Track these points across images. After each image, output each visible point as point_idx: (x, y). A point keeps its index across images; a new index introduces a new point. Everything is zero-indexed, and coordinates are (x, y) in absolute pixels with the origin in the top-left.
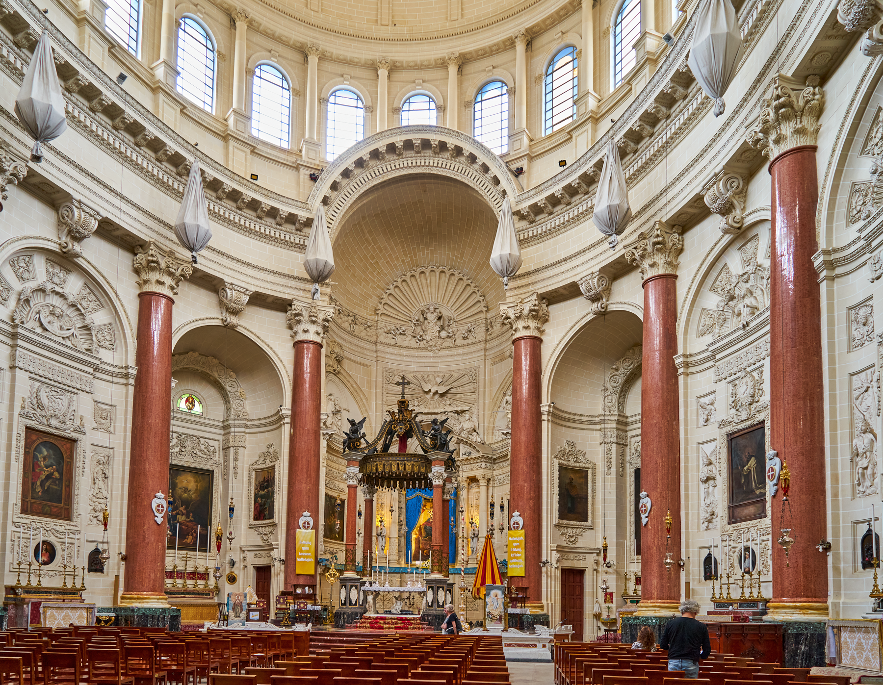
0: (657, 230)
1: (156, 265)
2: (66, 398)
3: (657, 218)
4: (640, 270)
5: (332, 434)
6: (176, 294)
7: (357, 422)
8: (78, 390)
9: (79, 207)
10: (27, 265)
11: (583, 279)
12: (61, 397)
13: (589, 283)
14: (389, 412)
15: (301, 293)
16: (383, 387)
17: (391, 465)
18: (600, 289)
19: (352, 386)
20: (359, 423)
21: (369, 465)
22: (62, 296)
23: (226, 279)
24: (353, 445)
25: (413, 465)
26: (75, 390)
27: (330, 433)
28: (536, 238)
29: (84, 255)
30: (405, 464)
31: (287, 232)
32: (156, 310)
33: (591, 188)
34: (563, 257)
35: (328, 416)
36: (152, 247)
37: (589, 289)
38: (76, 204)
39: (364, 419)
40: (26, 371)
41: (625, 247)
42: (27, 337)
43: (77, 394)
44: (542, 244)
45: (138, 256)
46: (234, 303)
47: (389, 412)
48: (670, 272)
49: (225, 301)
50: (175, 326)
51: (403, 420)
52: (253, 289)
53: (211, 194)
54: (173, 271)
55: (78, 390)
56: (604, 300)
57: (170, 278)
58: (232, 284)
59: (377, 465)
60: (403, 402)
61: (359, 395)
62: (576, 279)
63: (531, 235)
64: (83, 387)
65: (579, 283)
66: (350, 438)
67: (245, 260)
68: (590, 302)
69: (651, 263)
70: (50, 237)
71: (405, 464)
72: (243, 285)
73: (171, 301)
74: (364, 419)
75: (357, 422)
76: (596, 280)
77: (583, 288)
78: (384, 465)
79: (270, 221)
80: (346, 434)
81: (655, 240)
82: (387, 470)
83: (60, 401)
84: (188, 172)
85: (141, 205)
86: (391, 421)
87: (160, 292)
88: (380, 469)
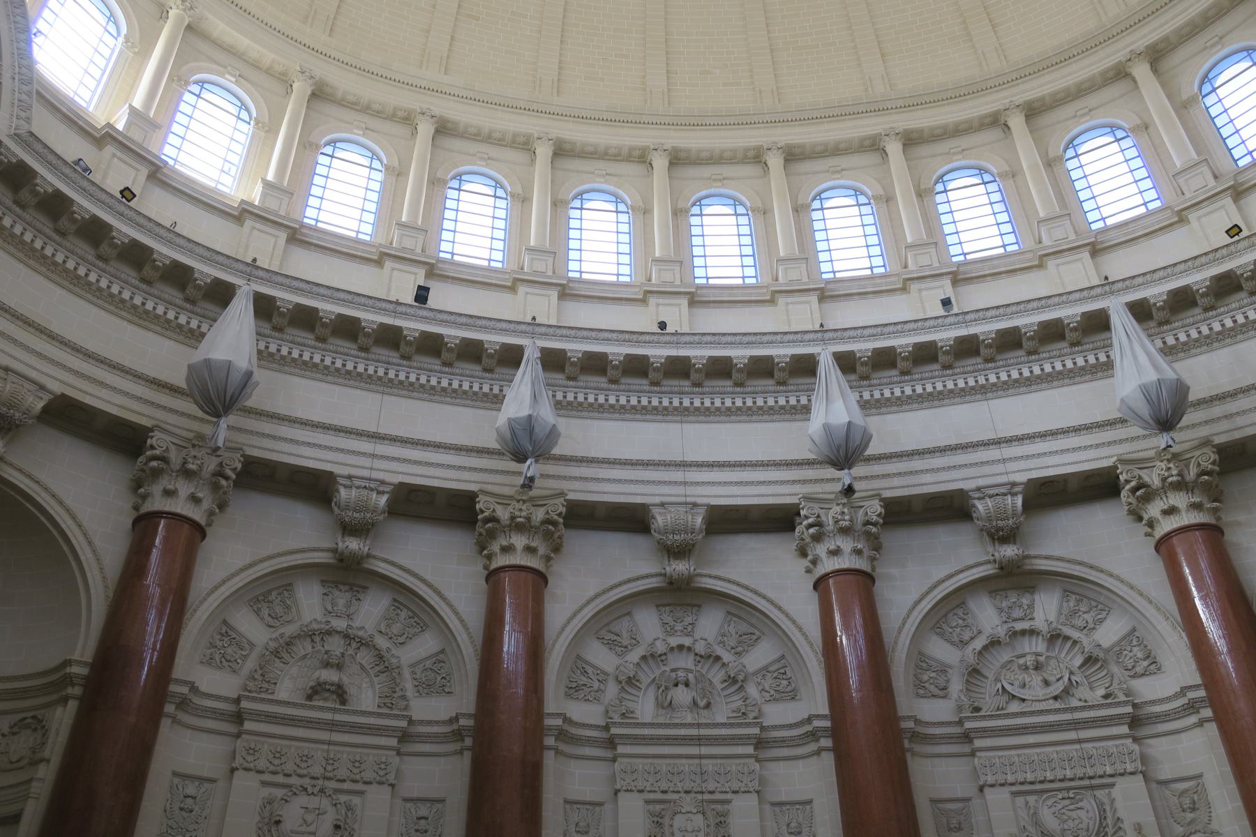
2: (1088, 803)
8: (1112, 776)
9: (982, 495)
10: (964, 620)
12: (1080, 804)
22: (994, 643)
26: (1104, 781)
29: (1032, 553)
38: (976, 496)
40: (1002, 785)
42: (984, 730)
43: (1112, 785)
55: (1112, 776)
64: (1120, 768)
70: (971, 562)
83: (1082, 813)
85: (1088, 421)
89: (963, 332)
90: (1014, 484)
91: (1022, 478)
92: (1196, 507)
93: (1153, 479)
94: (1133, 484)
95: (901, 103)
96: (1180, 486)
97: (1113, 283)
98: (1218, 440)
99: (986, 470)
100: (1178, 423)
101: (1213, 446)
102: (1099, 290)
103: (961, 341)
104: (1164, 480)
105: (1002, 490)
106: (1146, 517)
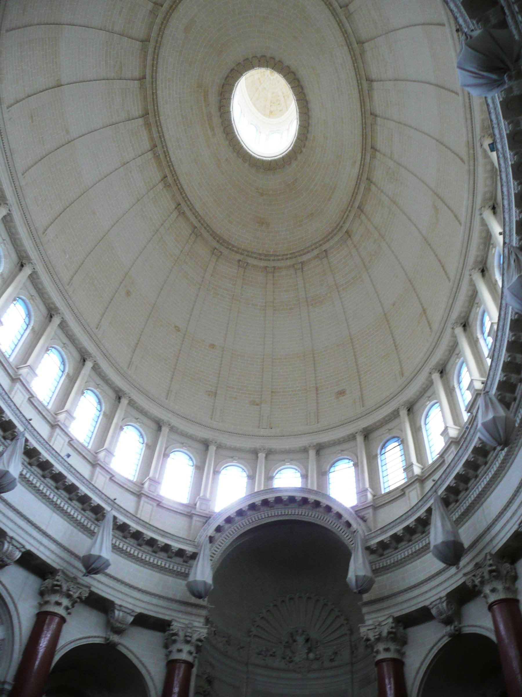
0: (490, 560)
1: (58, 588)
3: (487, 551)
4: (482, 595)
6: (69, 614)
11: (434, 603)
13: (438, 608)
15: (180, 615)
18: (450, 613)
23: (117, 602)
28: (387, 569)
31: (175, 564)
32: (48, 628)
33: (427, 529)
34: (412, 584)
36: (60, 573)
37: (440, 613)
41: (465, 575)
44: (392, 574)
45: (47, 581)
46: (120, 623)
48: (510, 596)
49: (112, 621)
50: (62, 642)
52: (139, 610)
53: (119, 534)
54: (71, 593)
56: (456, 623)
57: (68, 600)
58: (121, 606)
62: (427, 603)
63: (381, 566)
65: (431, 607)
67: (136, 585)
68: (442, 625)
69: (491, 589)
72: (130, 606)
73: (63, 620)
76: (444, 604)
77: (434, 612)
79: (163, 555)
81: (490, 568)
84: (104, 516)
87: (56, 611)
89: (65, 473)
90: (24, 547)
91: (28, 547)
92: (67, 608)
93: (65, 588)
94: (59, 583)
95: (105, 351)
96: (69, 596)
97: (115, 503)
98: (93, 589)
99: (20, 531)
100: (93, 574)
101: (90, 590)
102: (109, 501)
103: (60, 474)
104: (69, 590)
105: (19, 546)
106: (47, 598)
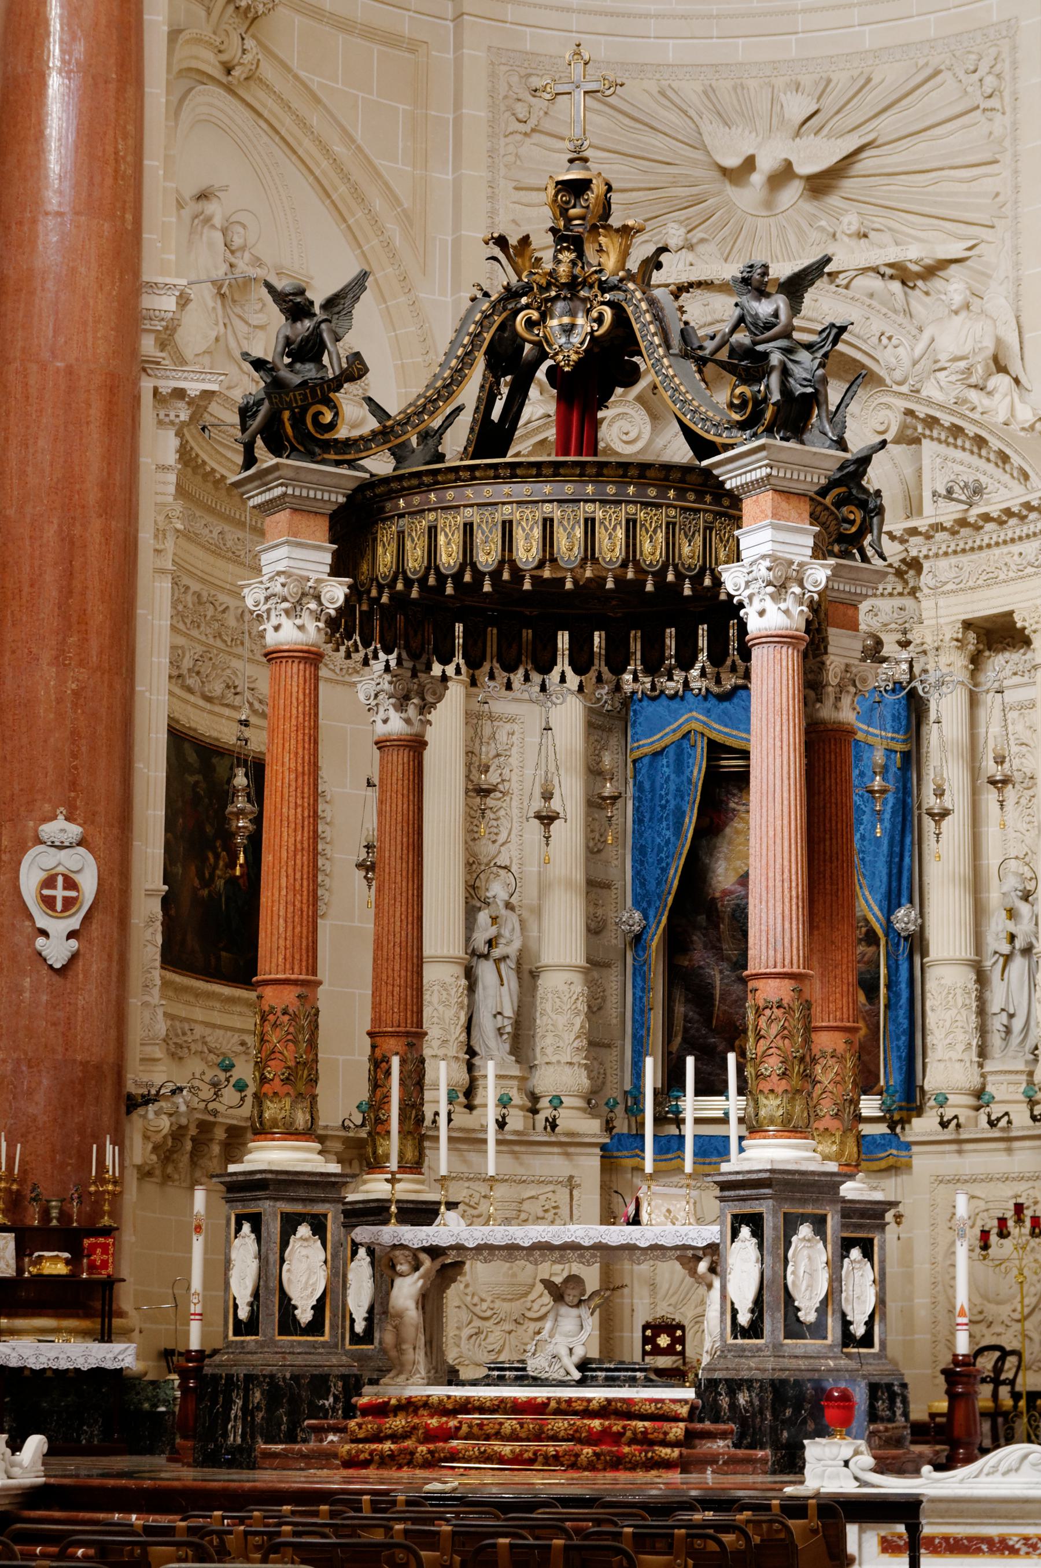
5: (208, 395)
7: (318, 296)
14: (501, 242)
16: (492, 153)
17: (507, 527)
19: (326, 151)
20: (330, 304)
21: (387, 534)
24: (298, 421)
25: (631, 524)
27: (194, 388)
30: (590, 524)
35: (184, 301)
39: (358, 285)
47: (501, 242)
51: (573, 285)
59: (432, 532)
60: (577, 188)
61: (361, 199)
66: (276, 386)
71: (590, 524)
74: (358, 285)
75: (318, 296)
78: (468, 528)
80: (259, 364)
82: (487, 557)
86: (511, 294)
88: (449, 556)
